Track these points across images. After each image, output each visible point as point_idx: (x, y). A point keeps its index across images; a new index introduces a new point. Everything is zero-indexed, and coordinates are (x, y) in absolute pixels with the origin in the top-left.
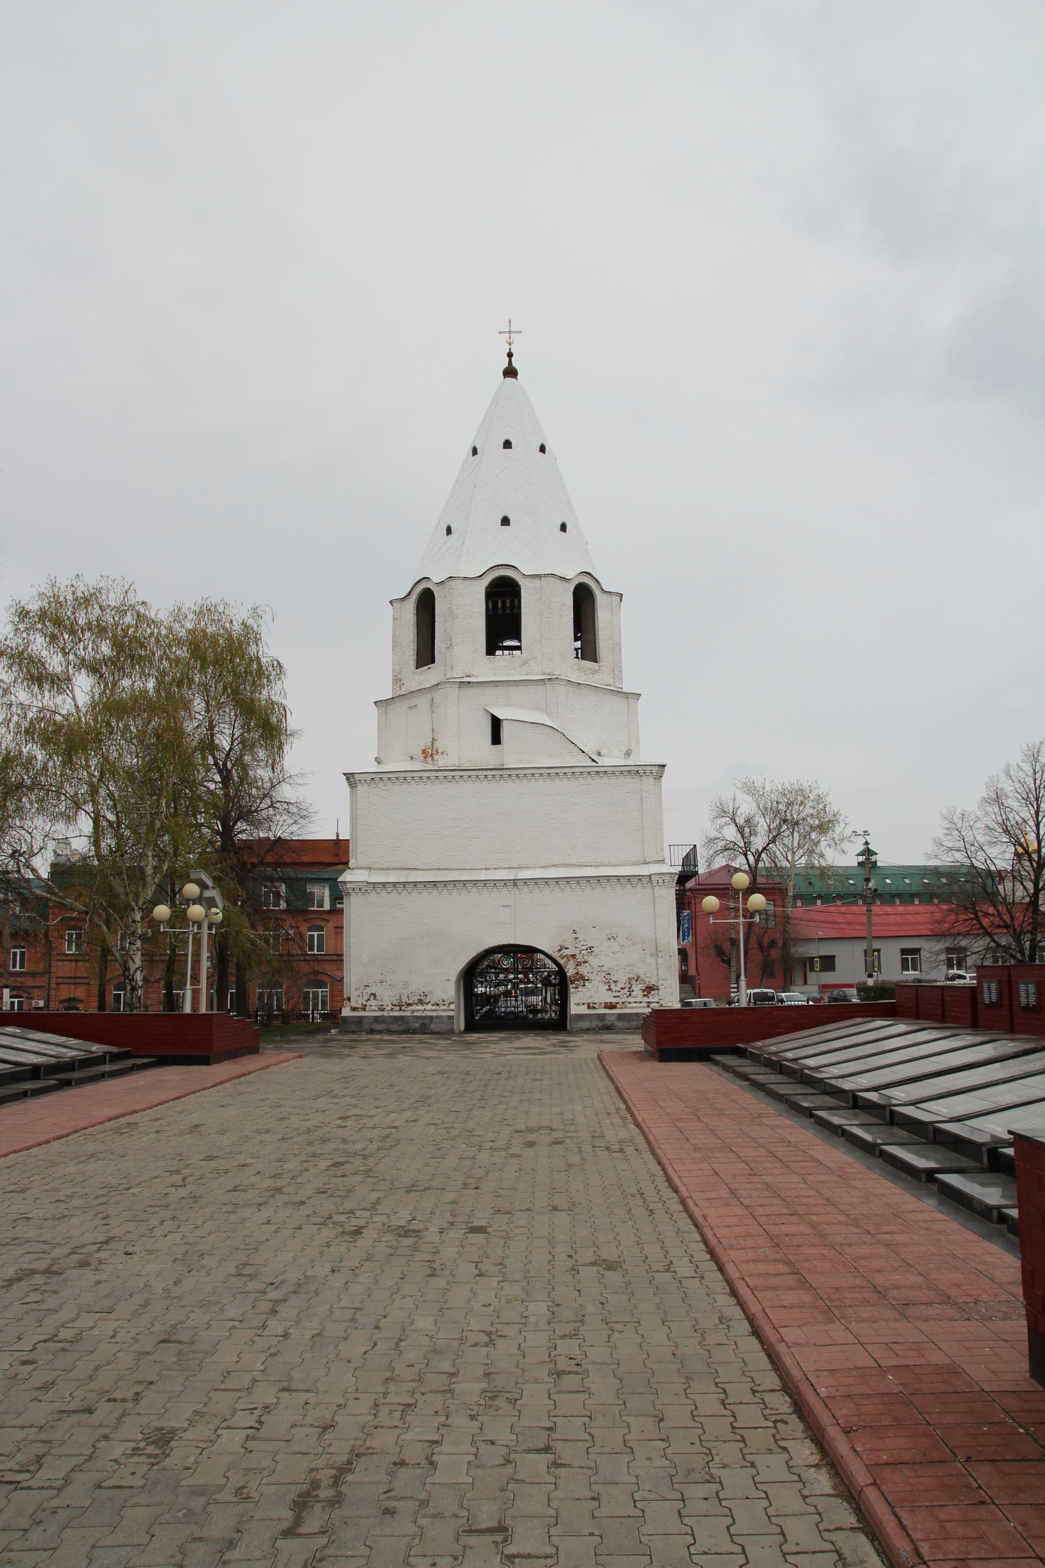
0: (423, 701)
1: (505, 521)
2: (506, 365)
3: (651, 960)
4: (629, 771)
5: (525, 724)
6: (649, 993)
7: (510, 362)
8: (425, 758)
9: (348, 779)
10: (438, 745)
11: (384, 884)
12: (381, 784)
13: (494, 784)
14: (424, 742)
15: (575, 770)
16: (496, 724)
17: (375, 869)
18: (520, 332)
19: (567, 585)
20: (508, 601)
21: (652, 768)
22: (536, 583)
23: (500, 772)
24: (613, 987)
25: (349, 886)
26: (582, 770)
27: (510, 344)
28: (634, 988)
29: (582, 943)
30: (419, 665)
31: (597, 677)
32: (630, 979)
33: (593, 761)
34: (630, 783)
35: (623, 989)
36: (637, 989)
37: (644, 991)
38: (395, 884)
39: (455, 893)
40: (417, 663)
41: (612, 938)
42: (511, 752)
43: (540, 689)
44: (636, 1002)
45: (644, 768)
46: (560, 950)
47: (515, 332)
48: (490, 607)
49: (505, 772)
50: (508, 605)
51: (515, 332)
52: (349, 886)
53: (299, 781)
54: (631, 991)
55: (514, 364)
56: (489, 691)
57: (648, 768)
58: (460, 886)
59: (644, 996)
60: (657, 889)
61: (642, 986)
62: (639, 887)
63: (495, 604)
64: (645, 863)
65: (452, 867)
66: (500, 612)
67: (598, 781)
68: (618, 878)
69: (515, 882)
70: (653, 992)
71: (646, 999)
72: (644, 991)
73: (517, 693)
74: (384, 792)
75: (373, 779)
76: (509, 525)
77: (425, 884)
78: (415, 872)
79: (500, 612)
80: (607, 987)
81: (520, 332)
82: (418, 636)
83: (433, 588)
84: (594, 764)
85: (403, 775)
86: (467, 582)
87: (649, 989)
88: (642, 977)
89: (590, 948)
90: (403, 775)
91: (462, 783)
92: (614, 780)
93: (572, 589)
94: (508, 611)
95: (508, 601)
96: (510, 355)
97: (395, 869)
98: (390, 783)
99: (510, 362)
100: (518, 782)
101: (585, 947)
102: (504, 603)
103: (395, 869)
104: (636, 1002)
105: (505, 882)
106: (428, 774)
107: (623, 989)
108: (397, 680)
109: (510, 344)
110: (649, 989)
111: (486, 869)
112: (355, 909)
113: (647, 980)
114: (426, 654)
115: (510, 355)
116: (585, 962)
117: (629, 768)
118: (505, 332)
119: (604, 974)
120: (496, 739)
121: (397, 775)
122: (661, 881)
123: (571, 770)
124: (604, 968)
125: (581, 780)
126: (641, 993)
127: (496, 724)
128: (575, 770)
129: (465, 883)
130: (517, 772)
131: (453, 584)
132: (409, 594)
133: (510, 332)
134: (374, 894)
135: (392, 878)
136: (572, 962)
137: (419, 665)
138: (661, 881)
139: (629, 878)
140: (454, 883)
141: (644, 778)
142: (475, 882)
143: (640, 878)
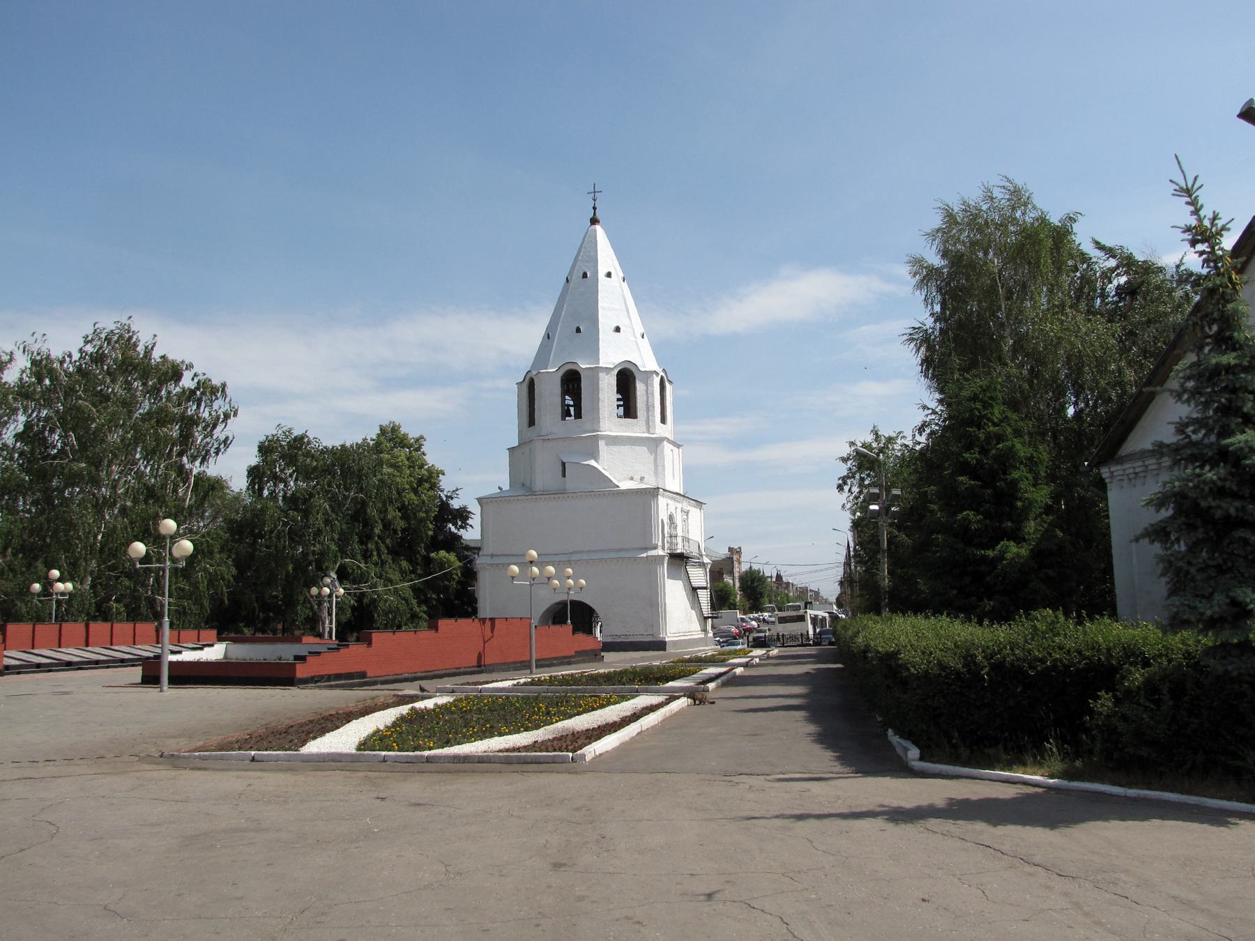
16: (564, 464)
23: (561, 492)
27: (595, 200)
30: (530, 426)
42: (571, 483)
48: (566, 389)
50: (576, 386)
96: (595, 208)
102: (573, 386)
109: (595, 200)
115: (595, 208)
120: (564, 475)
127: (564, 464)
132: (524, 380)
133: (595, 192)
137: (530, 426)
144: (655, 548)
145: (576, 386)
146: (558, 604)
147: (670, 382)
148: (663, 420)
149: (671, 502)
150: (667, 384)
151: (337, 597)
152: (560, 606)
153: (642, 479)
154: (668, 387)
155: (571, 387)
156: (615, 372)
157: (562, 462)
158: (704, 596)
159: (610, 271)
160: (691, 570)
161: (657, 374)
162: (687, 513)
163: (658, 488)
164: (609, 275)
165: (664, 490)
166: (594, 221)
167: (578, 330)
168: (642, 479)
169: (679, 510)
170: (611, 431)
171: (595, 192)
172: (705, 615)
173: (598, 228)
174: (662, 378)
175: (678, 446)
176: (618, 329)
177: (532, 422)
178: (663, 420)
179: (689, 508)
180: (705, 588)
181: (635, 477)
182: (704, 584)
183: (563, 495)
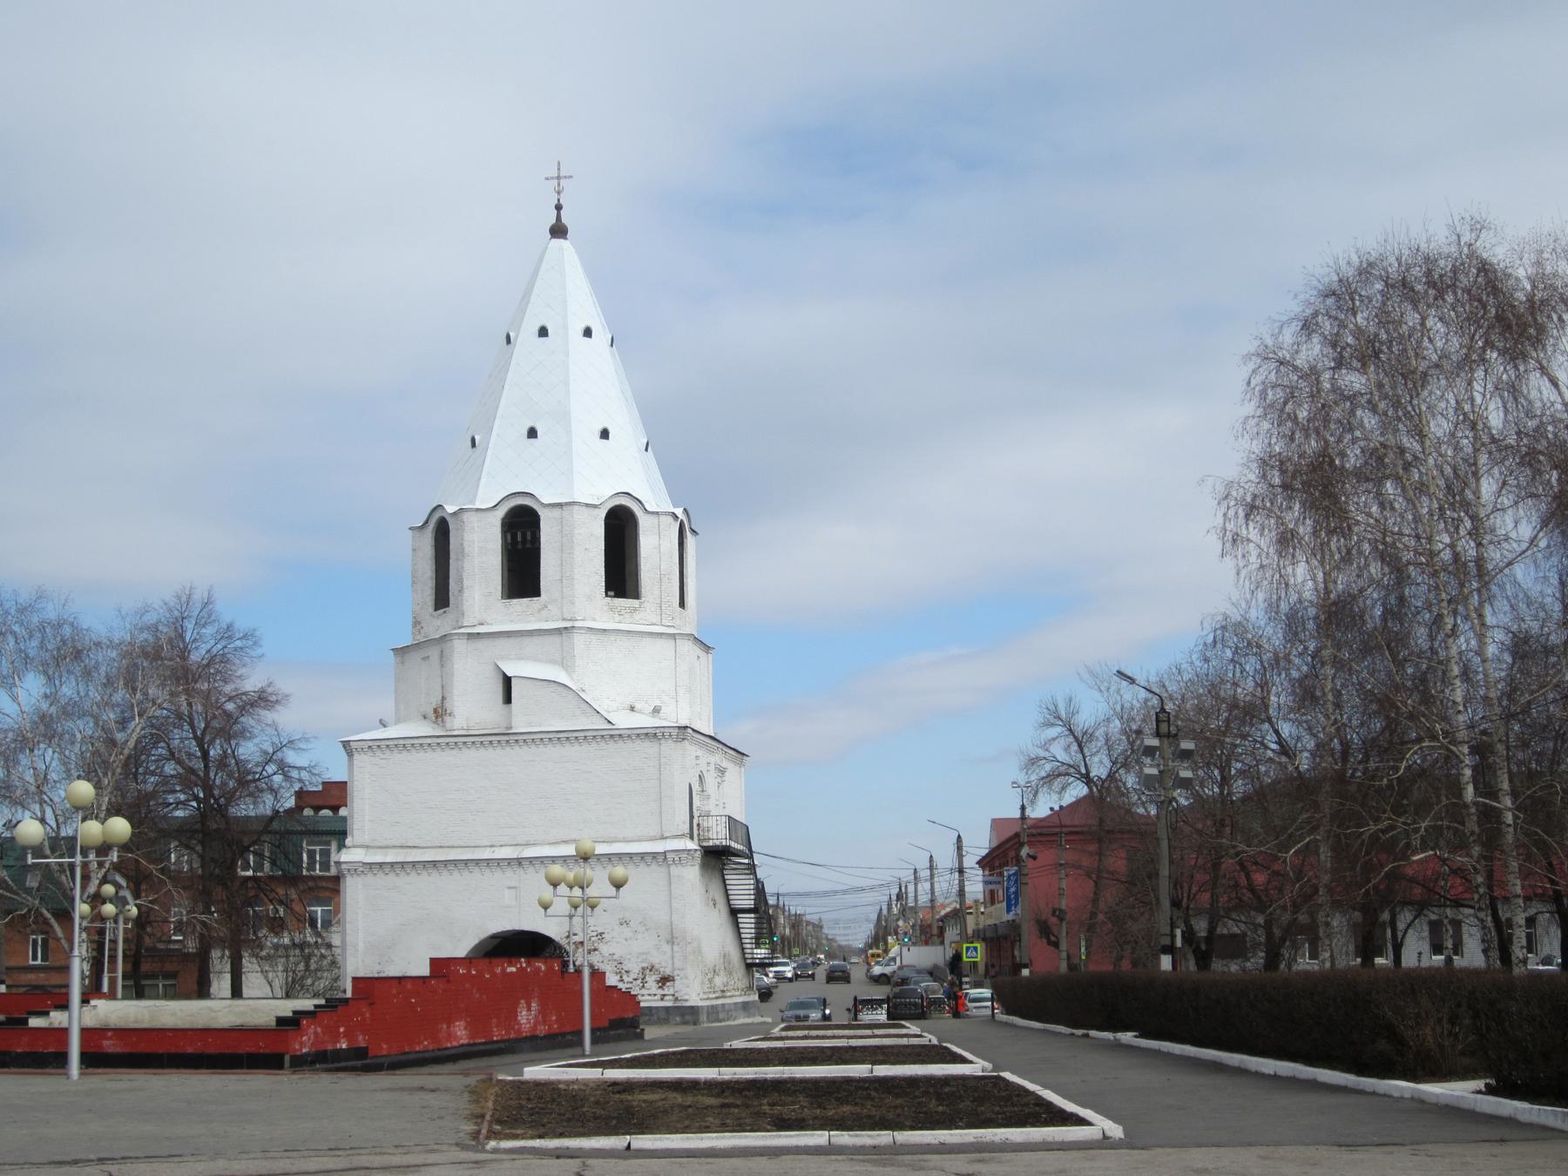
0: (434, 653)
1: (532, 433)
2: (554, 221)
3: (667, 948)
4: (647, 734)
5: (536, 682)
6: (664, 984)
7: (559, 217)
8: (437, 718)
9: (344, 747)
10: (447, 705)
11: (381, 865)
12: (378, 753)
13: (499, 750)
14: (435, 700)
15: (587, 734)
17: (373, 847)
18: (571, 177)
19: (596, 511)
20: (529, 534)
21: (671, 730)
22: (556, 512)
23: (506, 737)
24: (625, 977)
25: (344, 866)
26: (595, 733)
27: (559, 193)
28: (647, 979)
29: (592, 928)
31: (637, 616)
32: (643, 969)
33: (609, 722)
34: (648, 747)
35: (635, 979)
36: (651, 980)
37: (658, 982)
38: (392, 864)
39: (456, 874)
40: (436, 604)
41: (624, 923)
42: (524, 717)
43: (556, 639)
44: (649, 995)
45: (662, 730)
46: (568, 937)
47: (565, 177)
48: (509, 540)
49: (512, 737)
50: (529, 538)
51: (565, 177)
52: (344, 866)
53: (302, 746)
54: (644, 982)
55: (564, 220)
56: (501, 642)
57: (666, 730)
58: (461, 866)
59: (660, 987)
60: (673, 868)
61: (657, 977)
62: (654, 866)
63: (514, 537)
64: (663, 838)
65: (456, 845)
66: (520, 547)
67: (612, 746)
68: (631, 856)
69: (519, 862)
70: (668, 984)
71: (660, 992)
72: (658, 982)
73: (532, 644)
74: (384, 761)
75: (370, 747)
76: (536, 437)
77: (425, 864)
78: (415, 850)
79: (520, 547)
80: (618, 977)
81: (571, 177)
82: (436, 571)
83: (448, 519)
84: (611, 727)
85: (402, 742)
86: (480, 515)
87: (665, 980)
88: (657, 966)
89: (601, 934)
90: (402, 742)
91: (465, 750)
92: (630, 744)
93: (603, 515)
94: (528, 546)
95: (529, 534)
96: (559, 208)
97: (395, 847)
98: (388, 752)
99: (559, 217)
100: (525, 748)
101: (595, 934)
102: (524, 535)
103: (395, 847)
104: (649, 995)
105: (509, 861)
106: (429, 741)
107: (635, 979)
108: (416, 623)
109: (559, 193)
110: (665, 980)
111: (491, 846)
112: (355, 892)
113: (662, 969)
114: (442, 599)
115: (559, 208)
116: (595, 950)
117: (645, 731)
118: (552, 178)
119: (615, 963)
120: (508, 699)
121: (396, 742)
122: (677, 858)
123: (583, 734)
124: (615, 957)
125: (594, 744)
126: (655, 984)
127: (507, 681)
128: (587, 734)
129: (466, 862)
130: (525, 737)
131: (466, 516)
132: (427, 522)
133: (559, 178)
134: (370, 875)
135: (390, 857)
136: (580, 950)
138: (677, 858)
139: (642, 856)
140: (455, 862)
141: (663, 741)
142: (477, 862)
143: (654, 855)
145: (529, 538)
146: (494, 937)
147: (694, 532)
148: (682, 604)
149: (699, 753)
150: (688, 533)
151: (126, 921)
152: (498, 940)
153: (656, 710)
154: (690, 540)
155: (519, 539)
156: (603, 513)
157: (504, 675)
158: (748, 922)
160: (733, 879)
161: (675, 517)
162: (722, 771)
164: (588, 333)
165: (694, 730)
167: (532, 433)
168: (656, 710)
169: (712, 767)
170: (594, 620)
174: (682, 522)
175: (707, 648)
176: (605, 434)
177: (442, 599)
178: (682, 604)
179: (725, 764)
181: (638, 706)
183: (506, 738)
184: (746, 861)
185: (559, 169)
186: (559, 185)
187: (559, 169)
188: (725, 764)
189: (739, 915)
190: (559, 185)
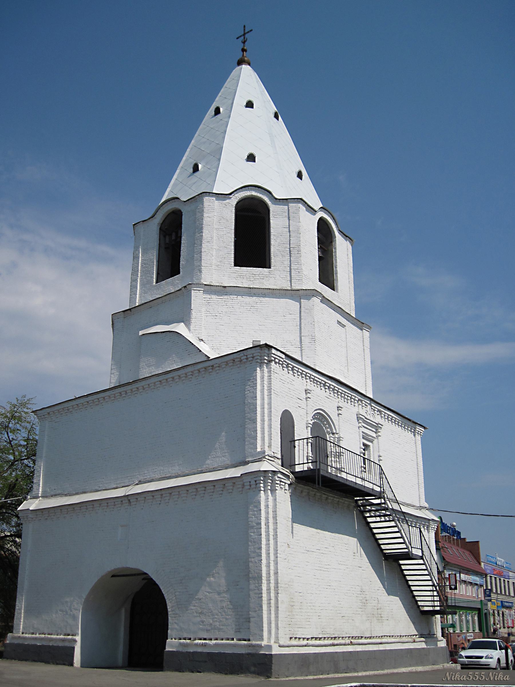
109: (244, 42)
122: (253, 482)
133: (244, 34)
144: (261, 458)
145: (179, 235)
156: (234, 201)
159: (251, 99)
162: (377, 427)
163: (269, 347)
164: (250, 105)
166: (240, 62)
167: (196, 168)
171: (244, 34)
172: (426, 609)
173: (245, 68)
179: (378, 419)
180: (408, 556)
182: (400, 548)
184: (377, 501)
185: (244, 30)
186: (244, 38)
187: (244, 30)
188: (378, 419)
189: (401, 562)
190: (244, 38)
